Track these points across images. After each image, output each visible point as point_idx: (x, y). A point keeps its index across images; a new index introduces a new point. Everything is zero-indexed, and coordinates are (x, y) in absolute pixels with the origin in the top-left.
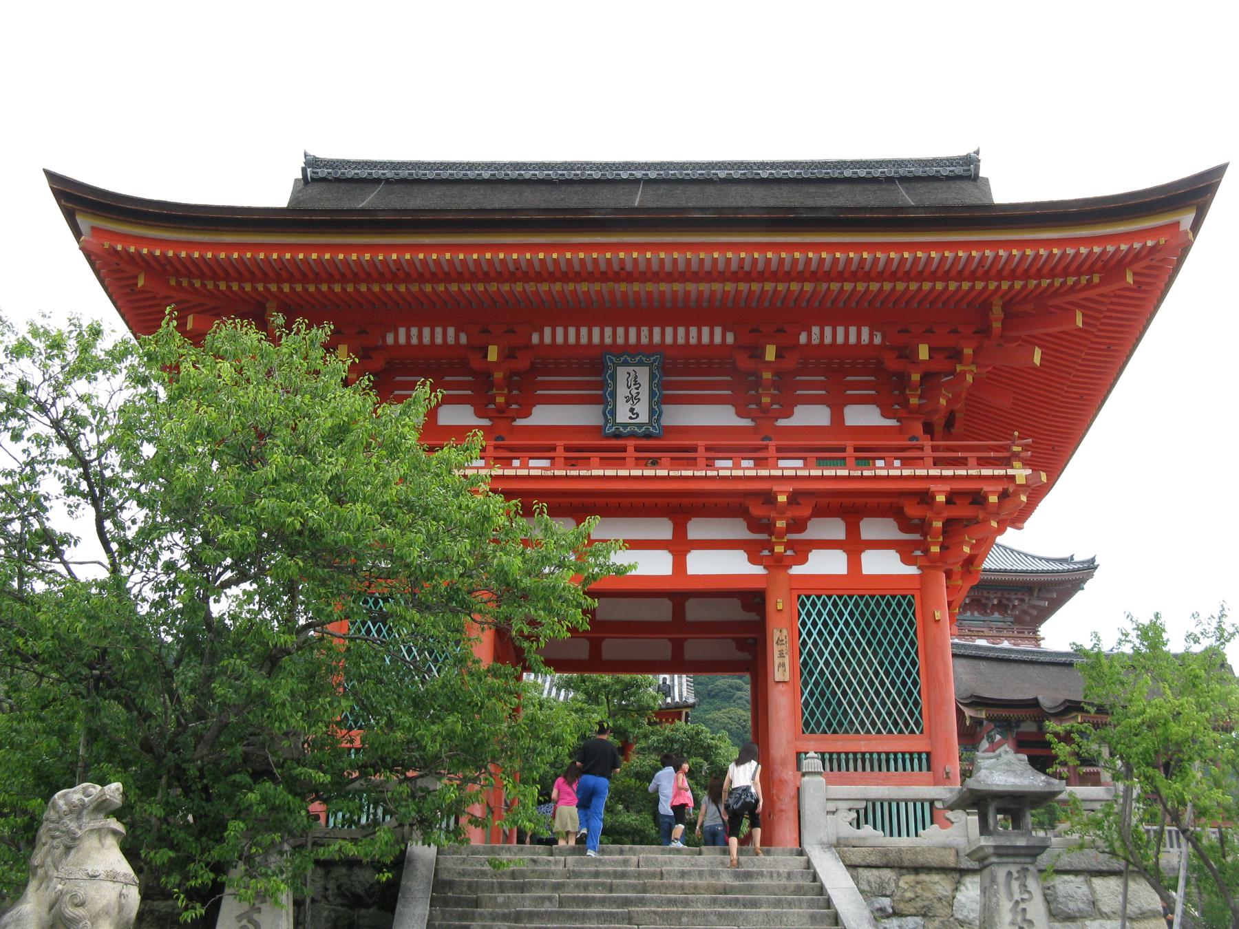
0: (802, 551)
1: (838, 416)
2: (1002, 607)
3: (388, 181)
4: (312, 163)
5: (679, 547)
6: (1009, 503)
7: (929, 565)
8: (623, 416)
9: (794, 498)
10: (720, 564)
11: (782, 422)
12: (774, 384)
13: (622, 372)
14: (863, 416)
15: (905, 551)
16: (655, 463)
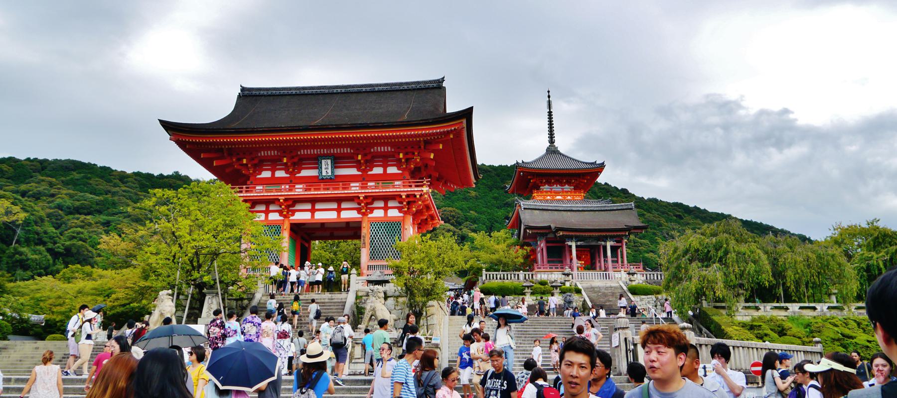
0: (372, 210)
1: (385, 170)
2: (569, 184)
3: (265, 96)
4: (243, 89)
5: (339, 210)
6: (423, 198)
7: (405, 213)
8: (324, 173)
9: (365, 197)
10: (350, 215)
11: (370, 173)
12: (366, 162)
13: (323, 161)
14: (392, 170)
15: (400, 209)
16: (328, 189)
